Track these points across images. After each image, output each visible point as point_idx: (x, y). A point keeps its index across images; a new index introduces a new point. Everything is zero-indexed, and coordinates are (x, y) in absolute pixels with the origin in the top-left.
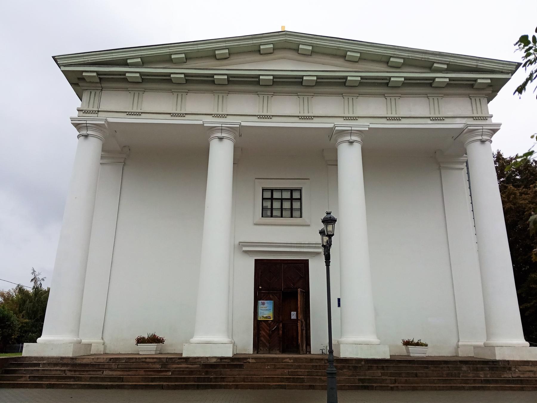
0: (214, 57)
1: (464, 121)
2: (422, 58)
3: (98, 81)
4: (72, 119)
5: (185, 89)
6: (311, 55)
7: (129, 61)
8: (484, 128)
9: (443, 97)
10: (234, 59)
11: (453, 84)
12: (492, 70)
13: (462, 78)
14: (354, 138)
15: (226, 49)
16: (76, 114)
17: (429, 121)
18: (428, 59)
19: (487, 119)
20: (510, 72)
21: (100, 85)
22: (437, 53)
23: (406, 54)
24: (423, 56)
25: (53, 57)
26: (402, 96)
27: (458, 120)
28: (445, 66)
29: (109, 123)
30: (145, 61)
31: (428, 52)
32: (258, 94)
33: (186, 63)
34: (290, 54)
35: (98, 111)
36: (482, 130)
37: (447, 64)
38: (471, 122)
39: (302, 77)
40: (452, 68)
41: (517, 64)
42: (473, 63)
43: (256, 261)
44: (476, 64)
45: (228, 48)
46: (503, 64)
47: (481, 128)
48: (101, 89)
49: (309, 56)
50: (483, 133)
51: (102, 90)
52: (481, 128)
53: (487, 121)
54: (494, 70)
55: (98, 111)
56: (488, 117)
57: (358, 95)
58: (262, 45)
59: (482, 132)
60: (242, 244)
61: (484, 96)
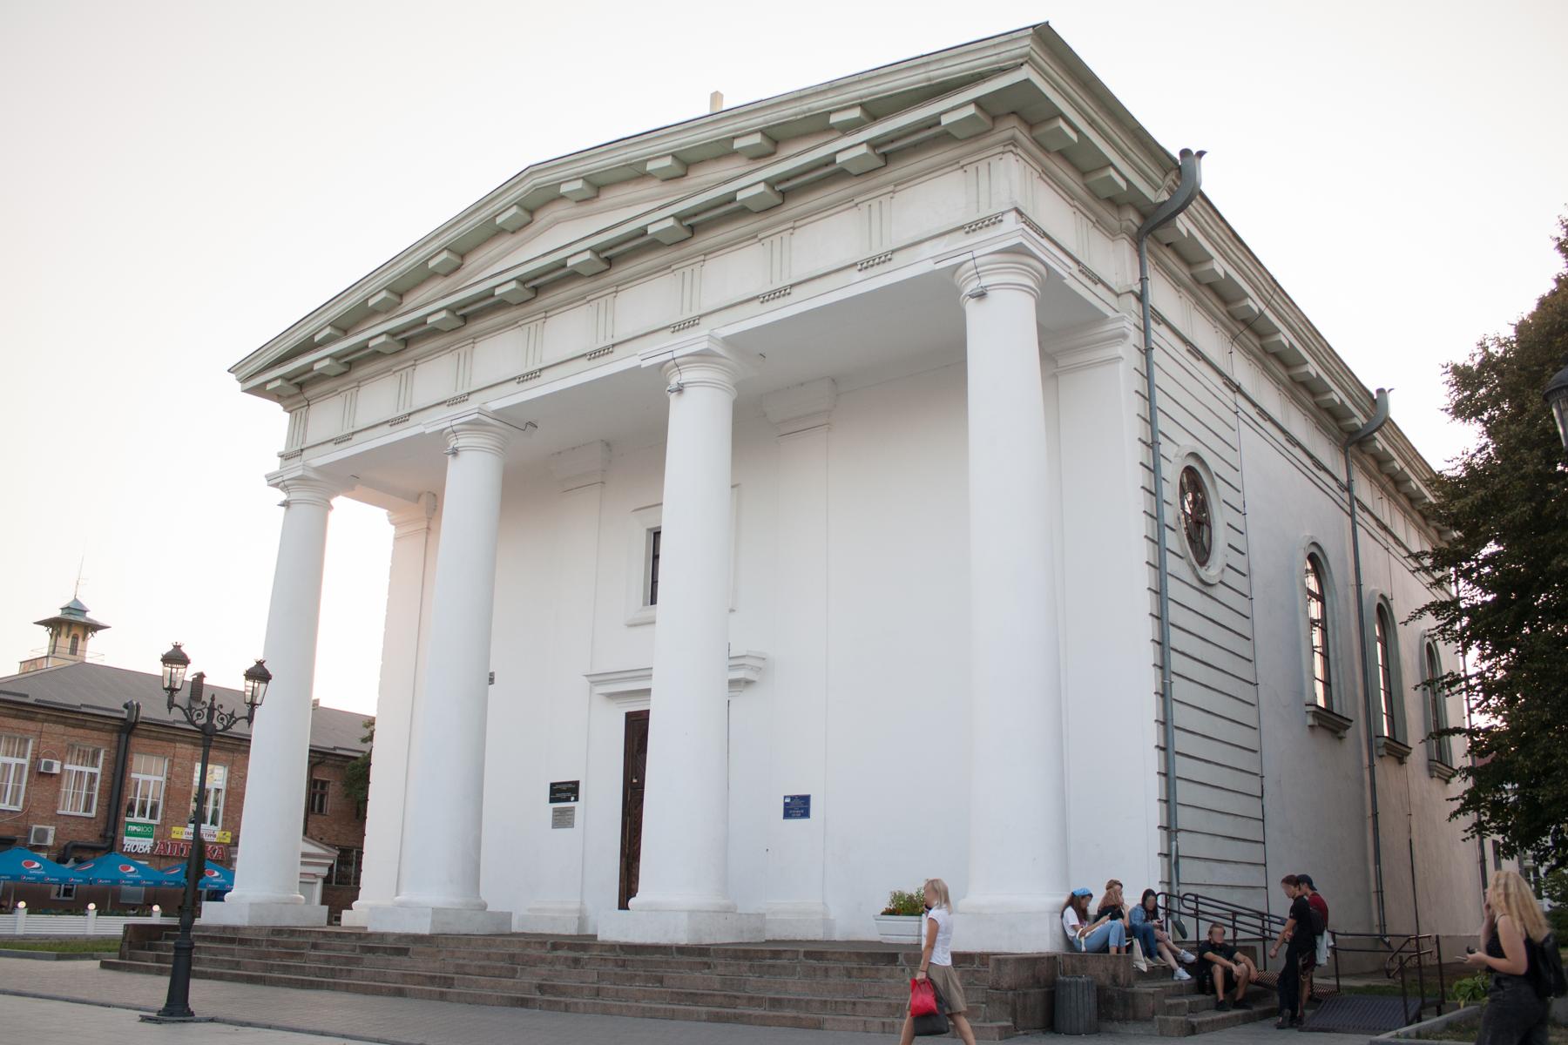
0: (433, 275)
1: (940, 247)
2: (796, 115)
3: (295, 390)
4: (269, 478)
5: (406, 361)
6: (598, 196)
7: (317, 338)
8: (976, 254)
9: (894, 192)
10: (473, 261)
11: (888, 153)
12: (972, 75)
13: (899, 129)
14: (688, 375)
15: (443, 250)
16: (275, 465)
17: (855, 275)
18: (810, 110)
19: (1001, 221)
20: (1021, 61)
21: (301, 397)
22: (824, 88)
23: (759, 120)
24: (797, 110)
25: (229, 371)
26: (798, 224)
27: (928, 249)
28: (856, 113)
29: (317, 470)
30: (343, 327)
31: (803, 93)
32: (520, 326)
33: (402, 305)
34: (559, 210)
35: (302, 450)
36: (972, 262)
37: (861, 105)
38: (961, 241)
39: (562, 265)
40: (874, 110)
41: (1031, 31)
42: (916, 79)
43: (629, 715)
44: (923, 76)
45: (446, 248)
46: (994, 46)
47: (969, 256)
48: (306, 403)
49: (596, 199)
50: (978, 270)
51: (309, 405)
52: (969, 256)
53: (1003, 224)
54: (979, 73)
55: (302, 450)
56: (1003, 213)
57: (702, 258)
58: (499, 214)
59: (976, 268)
60: (596, 679)
61: (1001, 149)
